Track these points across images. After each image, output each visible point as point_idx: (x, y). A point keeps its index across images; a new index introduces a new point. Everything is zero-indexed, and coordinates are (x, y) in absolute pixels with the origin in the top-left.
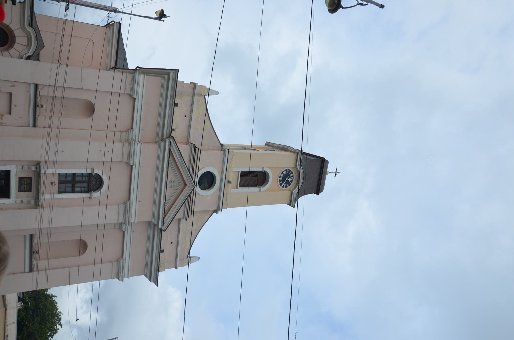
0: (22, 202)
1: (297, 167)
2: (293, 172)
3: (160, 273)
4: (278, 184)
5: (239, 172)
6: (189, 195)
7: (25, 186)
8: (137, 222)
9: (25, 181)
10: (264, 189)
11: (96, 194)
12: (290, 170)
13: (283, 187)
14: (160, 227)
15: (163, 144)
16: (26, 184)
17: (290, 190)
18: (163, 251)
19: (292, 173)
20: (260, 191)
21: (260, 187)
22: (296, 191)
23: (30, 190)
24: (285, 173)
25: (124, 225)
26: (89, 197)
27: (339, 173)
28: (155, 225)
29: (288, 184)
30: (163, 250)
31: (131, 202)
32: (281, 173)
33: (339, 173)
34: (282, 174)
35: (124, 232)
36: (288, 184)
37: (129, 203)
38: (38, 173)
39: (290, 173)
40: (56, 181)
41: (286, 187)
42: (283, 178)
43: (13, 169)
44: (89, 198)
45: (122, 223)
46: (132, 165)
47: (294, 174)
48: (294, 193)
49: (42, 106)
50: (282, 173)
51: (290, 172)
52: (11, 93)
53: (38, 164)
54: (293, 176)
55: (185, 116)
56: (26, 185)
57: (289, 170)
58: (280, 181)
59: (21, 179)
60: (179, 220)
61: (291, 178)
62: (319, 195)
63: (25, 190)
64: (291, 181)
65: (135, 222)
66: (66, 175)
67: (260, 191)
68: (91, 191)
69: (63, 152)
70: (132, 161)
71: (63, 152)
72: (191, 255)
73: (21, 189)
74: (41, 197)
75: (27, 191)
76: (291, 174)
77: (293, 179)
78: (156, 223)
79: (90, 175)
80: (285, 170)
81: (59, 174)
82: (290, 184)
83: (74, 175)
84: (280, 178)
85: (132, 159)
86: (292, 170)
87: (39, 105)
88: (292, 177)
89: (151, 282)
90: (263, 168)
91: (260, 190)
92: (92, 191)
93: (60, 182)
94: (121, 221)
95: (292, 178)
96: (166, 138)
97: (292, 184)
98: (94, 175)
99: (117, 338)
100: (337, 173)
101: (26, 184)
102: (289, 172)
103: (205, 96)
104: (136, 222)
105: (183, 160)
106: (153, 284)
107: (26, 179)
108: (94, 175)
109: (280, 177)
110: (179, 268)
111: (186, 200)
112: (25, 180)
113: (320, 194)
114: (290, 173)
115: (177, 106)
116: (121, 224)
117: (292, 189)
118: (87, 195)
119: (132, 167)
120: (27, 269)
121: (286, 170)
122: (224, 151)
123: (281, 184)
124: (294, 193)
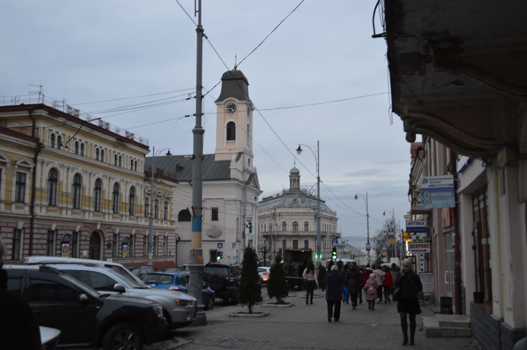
5: (227, 143)
10: (236, 125)
13: (236, 109)
19: (228, 105)
22: (238, 101)
29: (235, 106)
41: (236, 107)
47: (228, 103)
54: (230, 104)
58: (232, 113)
64: (233, 104)
67: (237, 126)
82: (234, 105)
86: (226, 106)
90: (224, 127)
97: (234, 103)
123: (235, 112)
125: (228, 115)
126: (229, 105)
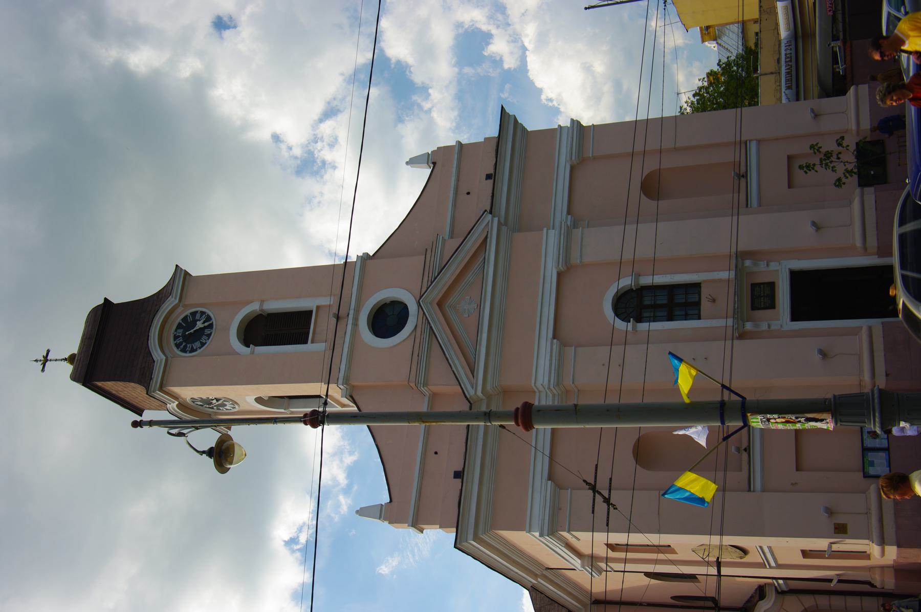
0: (768, 265)
1: (164, 358)
2: (175, 349)
3: (495, 133)
4: (215, 319)
5: (312, 342)
6: (432, 283)
7: (764, 292)
8: (543, 230)
9: (764, 303)
10: (254, 307)
11: (626, 282)
12: (184, 351)
13: (203, 313)
14: (496, 220)
15: (489, 387)
16: (762, 296)
17: (186, 306)
18: (489, 177)
19: (178, 346)
20: (262, 301)
21: (262, 310)
23: (754, 286)
24: (197, 344)
25: (569, 223)
26: (640, 277)
27: (36, 361)
28: (506, 224)
30: (486, 179)
31: (556, 268)
32: (206, 343)
33: (36, 361)
34: (204, 341)
35: (569, 213)
36: (190, 319)
37: (560, 266)
38: (739, 316)
39: (184, 344)
40: (705, 305)
41: (194, 314)
42: (199, 339)
43: (786, 324)
44: (639, 276)
45: (574, 228)
46: (555, 341)
48: (175, 298)
49: (738, 450)
50: (203, 344)
51: (182, 347)
52: (798, 469)
53: (742, 336)
54: (176, 338)
55: (436, 453)
56: (762, 295)
57: (185, 352)
58: (211, 326)
59: (772, 305)
60: (452, 235)
61: (180, 334)
62: (106, 299)
63: (762, 286)
64: (179, 326)
65: (547, 230)
66: (686, 317)
68: (637, 290)
69: (694, 359)
70: (554, 347)
71: (694, 359)
72: (428, 171)
73: (772, 286)
74: (733, 275)
75: (760, 284)
76: (180, 344)
77: (176, 331)
78: (504, 229)
79: (639, 320)
80: (196, 350)
81: (699, 318)
82: (185, 319)
83: (670, 318)
84: (209, 332)
85: (554, 351)
87: (744, 452)
88: (179, 337)
89: (515, 116)
90: (252, 353)
91: (261, 305)
92: (634, 289)
93: (698, 304)
94: (577, 232)
95: (178, 334)
96: (482, 400)
97: (179, 320)
98: (632, 319)
99: (586, 8)
100: (43, 359)
101: (762, 296)
102: (185, 347)
103: (391, 501)
104: (545, 230)
105: (446, 353)
106: (510, 110)
107: (762, 306)
108: (632, 319)
109: (209, 336)
110: (454, 144)
111: (438, 275)
112: (764, 305)
113: (102, 302)
114: (184, 344)
115: (455, 472)
116: (575, 225)
117: (180, 309)
118: (646, 281)
119: (554, 337)
120: (753, 147)
121: (193, 350)
122: (346, 384)
123: (209, 318)
124: (175, 298)
125: (212, 344)
126: (180, 340)
